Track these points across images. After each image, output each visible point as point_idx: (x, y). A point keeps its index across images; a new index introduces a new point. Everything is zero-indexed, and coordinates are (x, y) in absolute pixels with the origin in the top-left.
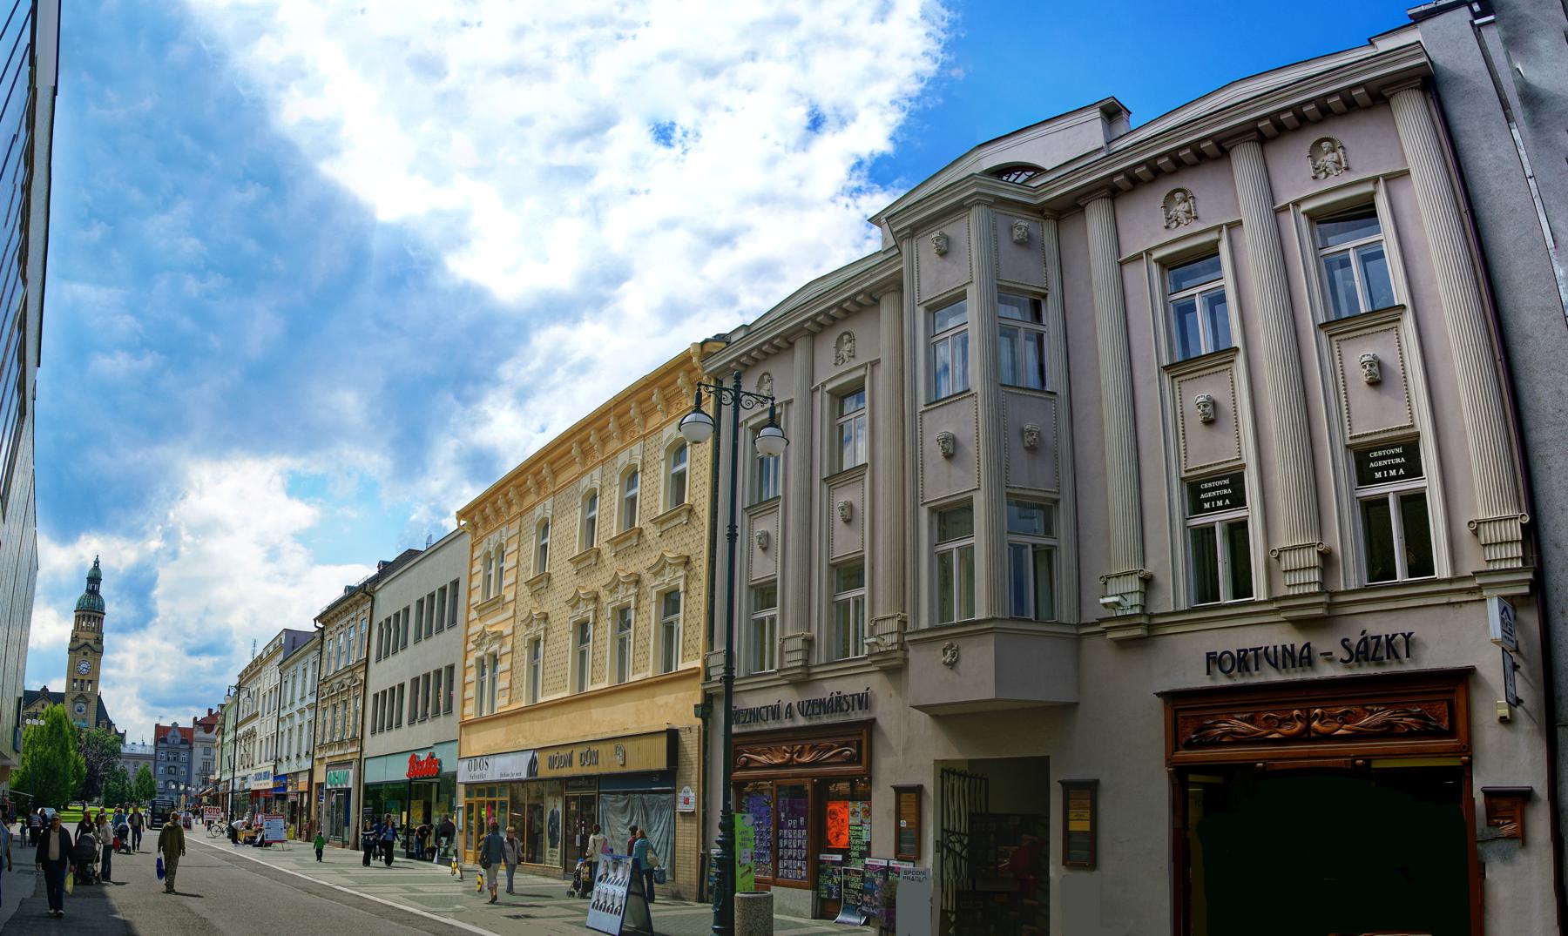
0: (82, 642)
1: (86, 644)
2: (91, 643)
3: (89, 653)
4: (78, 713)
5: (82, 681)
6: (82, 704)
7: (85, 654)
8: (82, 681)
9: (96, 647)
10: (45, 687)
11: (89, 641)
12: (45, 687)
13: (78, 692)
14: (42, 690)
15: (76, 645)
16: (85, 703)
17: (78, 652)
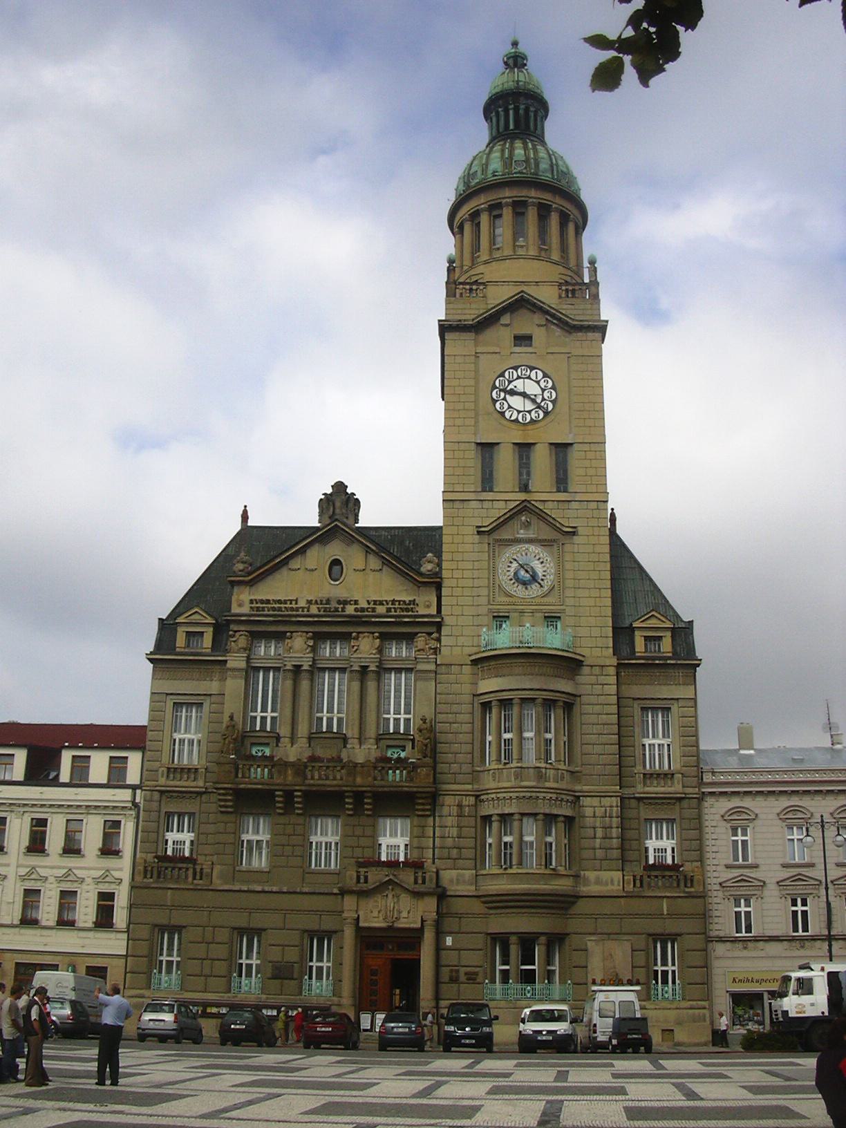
0: (498, 295)
1: (521, 304)
2: (547, 295)
3: (539, 335)
4: (519, 591)
5: (524, 449)
6: (532, 548)
7: (523, 340)
8: (524, 449)
9: (573, 311)
10: (340, 487)
11: (525, 288)
12: (340, 487)
13: (506, 496)
14: (327, 503)
15: (471, 311)
16: (545, 543)
17: (490, 334)
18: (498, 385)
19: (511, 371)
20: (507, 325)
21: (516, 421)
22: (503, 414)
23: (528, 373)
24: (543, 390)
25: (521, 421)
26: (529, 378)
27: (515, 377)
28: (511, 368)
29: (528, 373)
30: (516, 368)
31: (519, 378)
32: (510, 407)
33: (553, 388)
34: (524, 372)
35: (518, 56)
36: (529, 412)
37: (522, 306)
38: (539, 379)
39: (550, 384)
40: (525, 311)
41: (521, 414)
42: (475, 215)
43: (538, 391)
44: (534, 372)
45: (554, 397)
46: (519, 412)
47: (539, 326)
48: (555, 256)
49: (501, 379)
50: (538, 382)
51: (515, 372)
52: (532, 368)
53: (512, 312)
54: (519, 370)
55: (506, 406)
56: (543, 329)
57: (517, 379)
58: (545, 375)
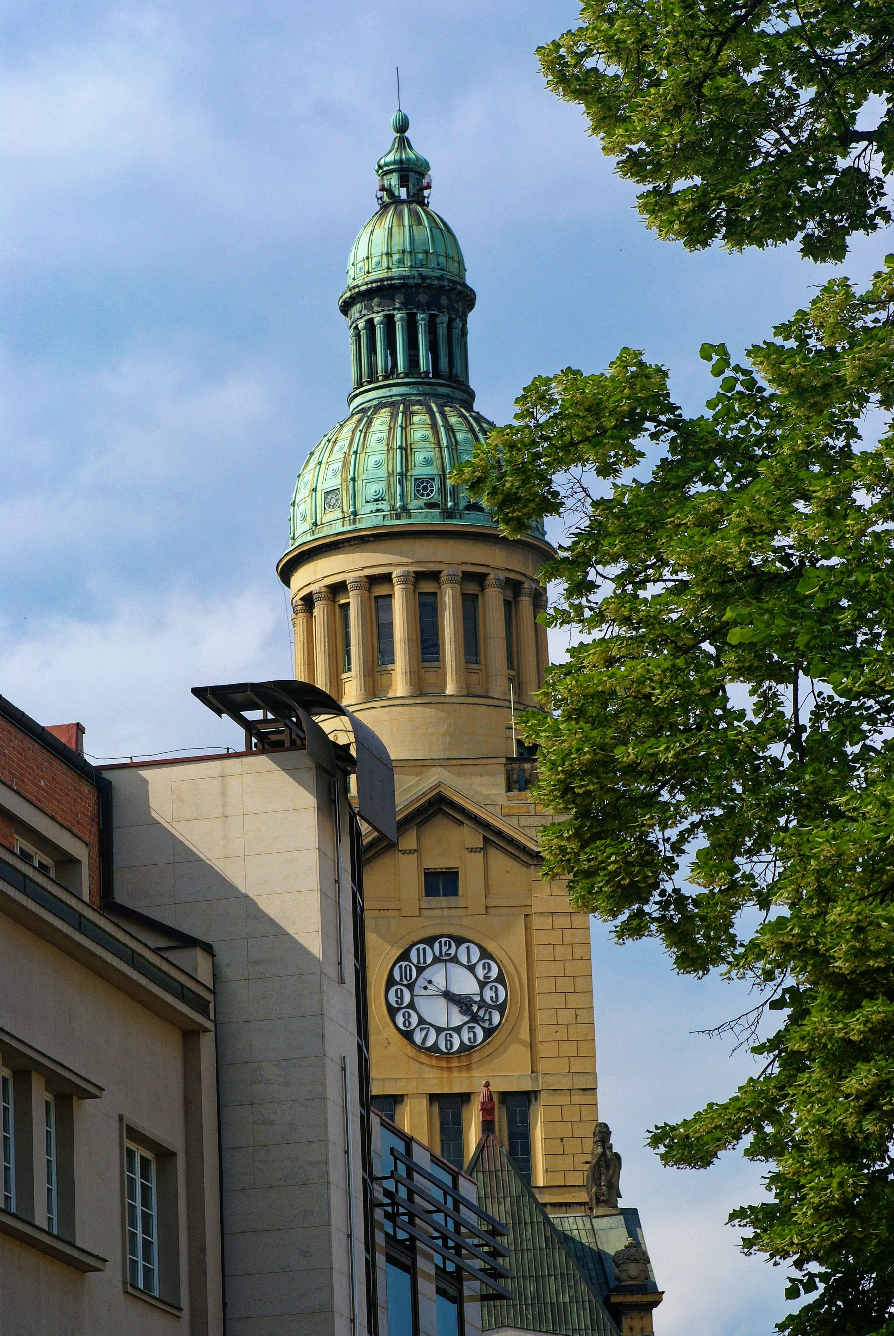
18: (398, 978)
19: (421, 946)
20: (409, 852)
21: (435, 1048)
22: (408, 1035)
23: (453, 951)
24: (482, 985)
25: (444, 1049)
26: (455, 960)
27: (429, 961)
28: (421, 942)
29: (453, 951)
30: (429, 941)
31: (436, 960)
32: (422, 1021)
33: (500, 979)
34: (444, 949)
35: (409, 170)
36: (458, 1030)
37: (440, 811)
38: (474, 961)
39: (494, 974)
40: (447, 822)
41: (442, 1035)
42: (338, 589)
43: (473, 987)
44: (463, 947)
45: (501, 999)
46: (439, 1030)
47: (472, 850)
48: (500, 686)
49: (404, 964)
50: (471, 968)
51: (428, 949)
52: (460, 941)
53: (419, 825)
54: (436, 945)
55: (414, 1020)
56: (480, 856)
57: (431, 964)
58: (485, 954)
